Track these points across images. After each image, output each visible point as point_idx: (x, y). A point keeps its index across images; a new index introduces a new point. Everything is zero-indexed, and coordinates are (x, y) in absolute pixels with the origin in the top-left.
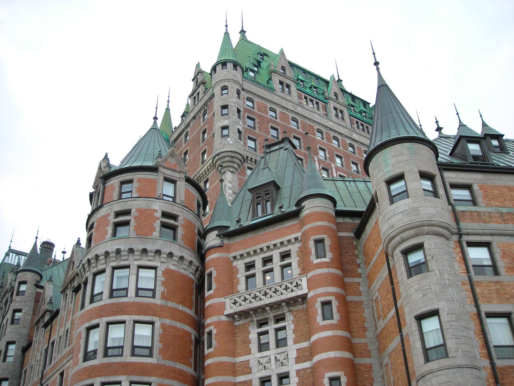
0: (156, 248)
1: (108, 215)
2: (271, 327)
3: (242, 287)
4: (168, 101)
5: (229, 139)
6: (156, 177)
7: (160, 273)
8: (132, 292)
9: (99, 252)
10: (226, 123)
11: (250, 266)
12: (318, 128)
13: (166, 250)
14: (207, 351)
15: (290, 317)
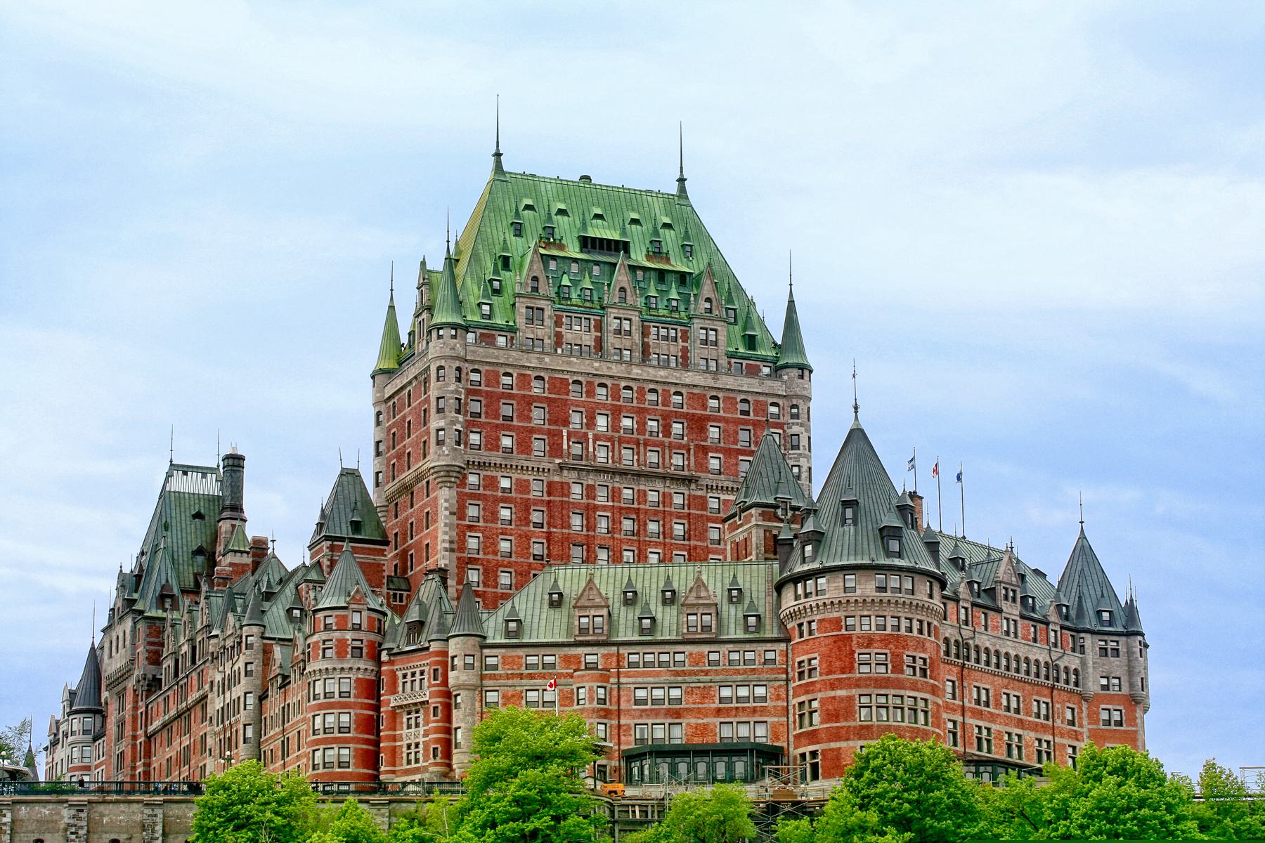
0: (349, 666)
1: (319, 642)
2: (413, 715)
3: (400, 689)
4: (392, 290)
5: (444, 448)
6: (346, 613)
7: (352, 681)
8: (337, 695)
9: (315, 668)
10: (442, 424)
11: (405, 676)
12: (575, 378)
13: (356, 666)
14: (381, 728)
15: (422, 711)
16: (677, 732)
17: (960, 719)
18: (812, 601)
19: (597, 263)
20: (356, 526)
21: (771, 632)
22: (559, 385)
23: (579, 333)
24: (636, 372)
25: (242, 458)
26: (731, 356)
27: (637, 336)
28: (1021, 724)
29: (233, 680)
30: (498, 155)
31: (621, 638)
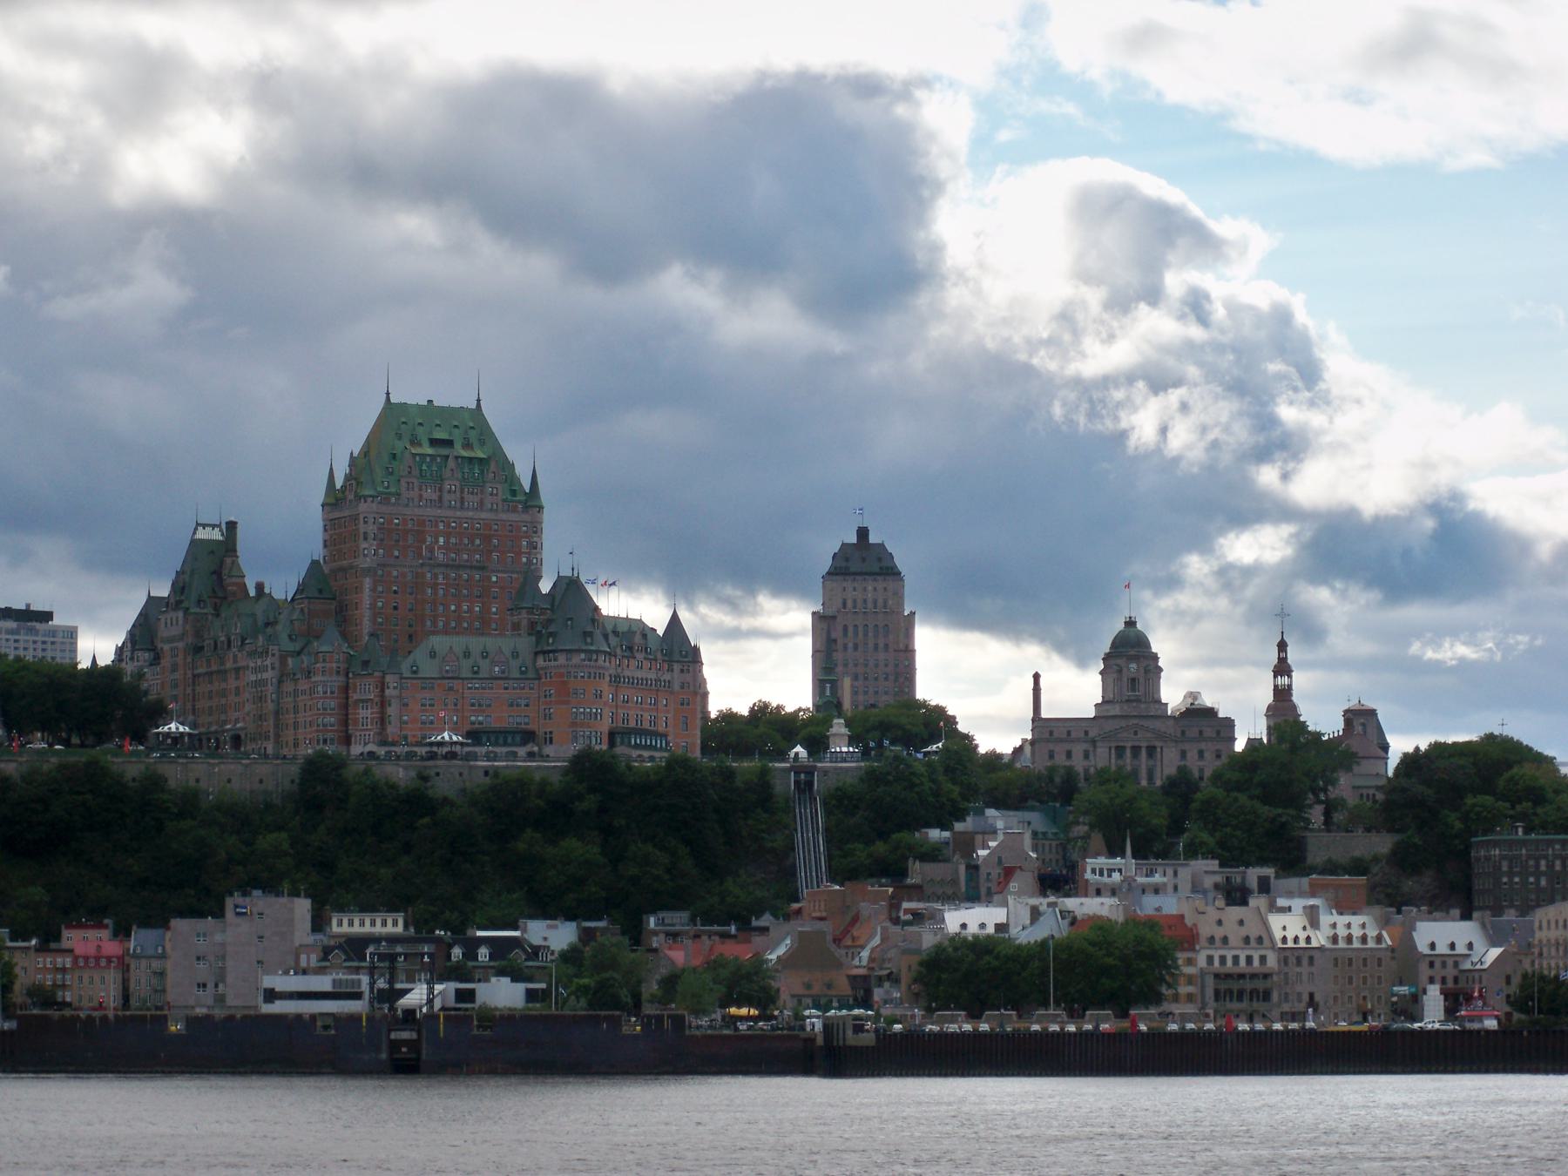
3: (358, 691)
11: (361, 685)
16: (489, 719)
17: (614, 711)
18: (553, 663)
19: (439, 456)
20: (320, 591)
21: (531, 675)
22: (422, 523)
23: (429, 493)
24: (459, 514)
25: (235, 523)
26: (505, 500)
27: (458, 493)
28: (642, 710)
29: (264, 669)
30: (388, 394)
31: (464, 676)
